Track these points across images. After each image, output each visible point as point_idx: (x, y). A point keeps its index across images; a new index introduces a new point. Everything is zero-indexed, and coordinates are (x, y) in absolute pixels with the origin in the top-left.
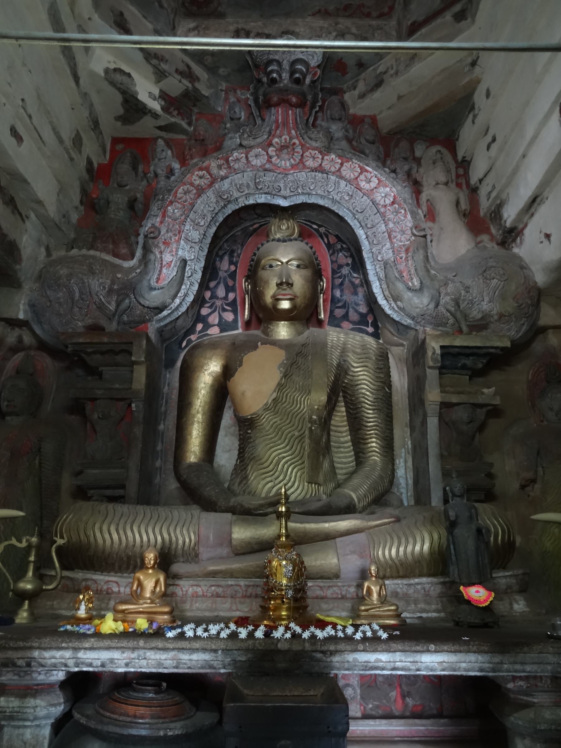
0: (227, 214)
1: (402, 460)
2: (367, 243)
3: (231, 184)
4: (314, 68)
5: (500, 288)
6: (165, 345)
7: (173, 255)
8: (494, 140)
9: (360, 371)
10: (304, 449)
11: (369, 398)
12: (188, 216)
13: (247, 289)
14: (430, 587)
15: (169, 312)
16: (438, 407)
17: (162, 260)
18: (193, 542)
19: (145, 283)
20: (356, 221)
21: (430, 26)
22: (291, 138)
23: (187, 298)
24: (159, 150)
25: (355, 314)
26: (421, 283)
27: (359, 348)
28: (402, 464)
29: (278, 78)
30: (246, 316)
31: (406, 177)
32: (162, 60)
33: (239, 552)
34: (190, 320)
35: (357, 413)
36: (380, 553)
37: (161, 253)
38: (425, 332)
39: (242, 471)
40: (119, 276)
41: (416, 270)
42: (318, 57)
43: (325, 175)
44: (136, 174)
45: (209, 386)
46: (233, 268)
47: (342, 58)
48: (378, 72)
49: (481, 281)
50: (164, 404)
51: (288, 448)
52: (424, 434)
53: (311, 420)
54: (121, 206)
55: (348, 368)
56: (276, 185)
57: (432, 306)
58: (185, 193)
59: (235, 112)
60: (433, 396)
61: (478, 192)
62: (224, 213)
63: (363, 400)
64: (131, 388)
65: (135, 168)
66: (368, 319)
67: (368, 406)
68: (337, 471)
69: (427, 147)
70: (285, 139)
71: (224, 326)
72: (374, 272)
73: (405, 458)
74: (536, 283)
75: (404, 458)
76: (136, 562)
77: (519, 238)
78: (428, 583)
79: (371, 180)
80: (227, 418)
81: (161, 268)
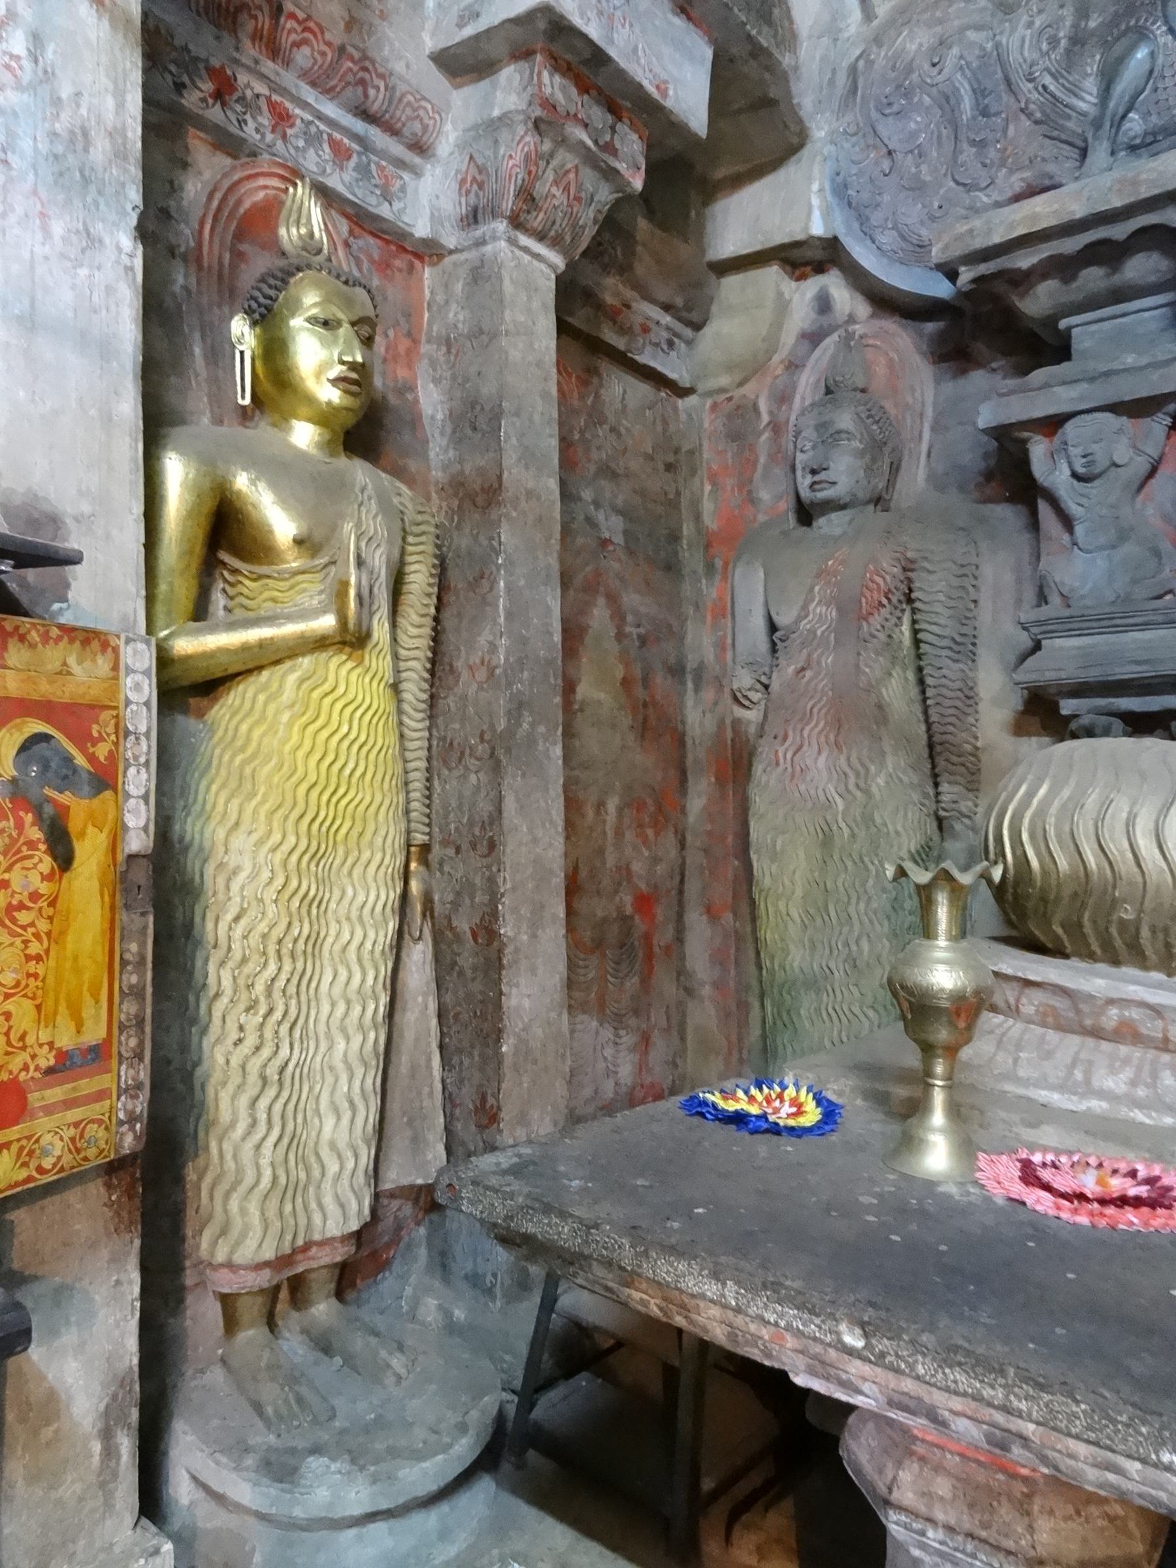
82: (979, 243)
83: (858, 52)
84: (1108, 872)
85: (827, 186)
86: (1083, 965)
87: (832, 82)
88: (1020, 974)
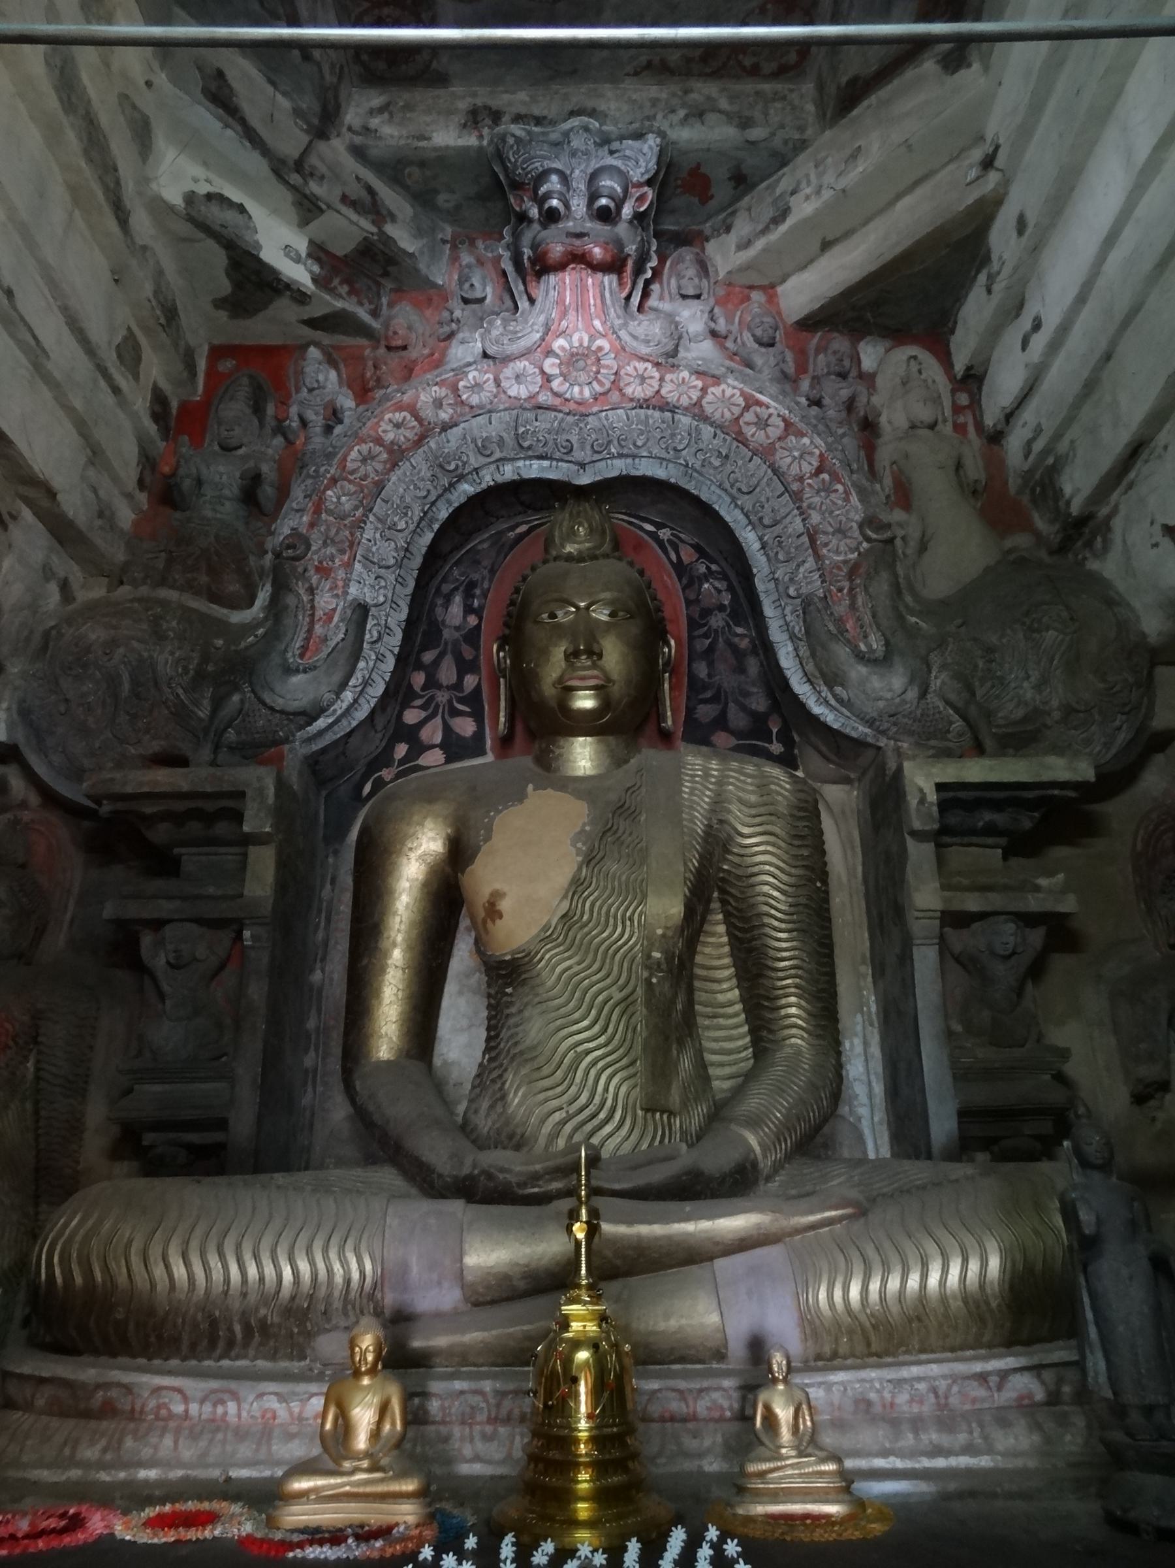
0: (456, 505)
1: (857, 1042)
2: (764, 559)
3: (465, 438)
4: (639, 185)
5: (1063, 648)
6: (324, 793)
7: (337, 596)
8: (1037, 326)
9: (757, 845)
10: (635, 1029)
11: (779, 906)
12: (371, 510)
13: (503, 666)
14: (949, 1387)
15: (330, 720)
16: (938, 922)
17: (313, 608)
18: (369, 1280)
19: (275, 659)
20: (737, 512)
21: (890, 87)
22: (592, 339)
23: (369, 690)
24: (310, 369)
25: (742, 714)
26: (887, 644)
27: (752, 792)
28: (859, 1049)
29: (562, 208)
30: (501, 727)
31: (844, 414)
32: (312, 175)
33: (481, 1299)
34: (380, 735)
35: (754, 939)
36: (822, 1295)
37: (311, 591)
38: (898, 752)
39: (493, 1081)
40: (220, 642)
41: (874, 616)
42: (648, 163)
43: (668, 414)
44: (262, 424)
45: (418, 884)
46: (473, 620)
47: (699, 165)
48: (778, 191)
49: (1021, 635)
50: (322, 924)
51: (597, 1028)
52: (908, 985)
54: (226, 492)
55: (730, 839)
56: (560, 439)
57: (912, 694)
58: (364, 460)
59: (472, 285)
60: (926, 897)
61: (1004, 442)
62: (449, 502)
63: (766, 908)
64: (241, 896)
65: (258, 409)
66: (771, 725)
67: (776, 923)
68: (711, 1071)
69: (888, 351)
70: (581, 340)
71: (455, 748)
72: (782, 622)
73: (864, 1037)
74: (1144, 635)
75: (861, 1035)
76: (230, 1330)
77: (1099, 539)
78: (944, 1377)
79: (769, 422)
81: (312, 623)
82: (117, 789)
83: (52, 623)
84: (109, 1284)
85: (14, 707)
86: (92, 1359)
87: (28, 640)
88: (36, 1373)
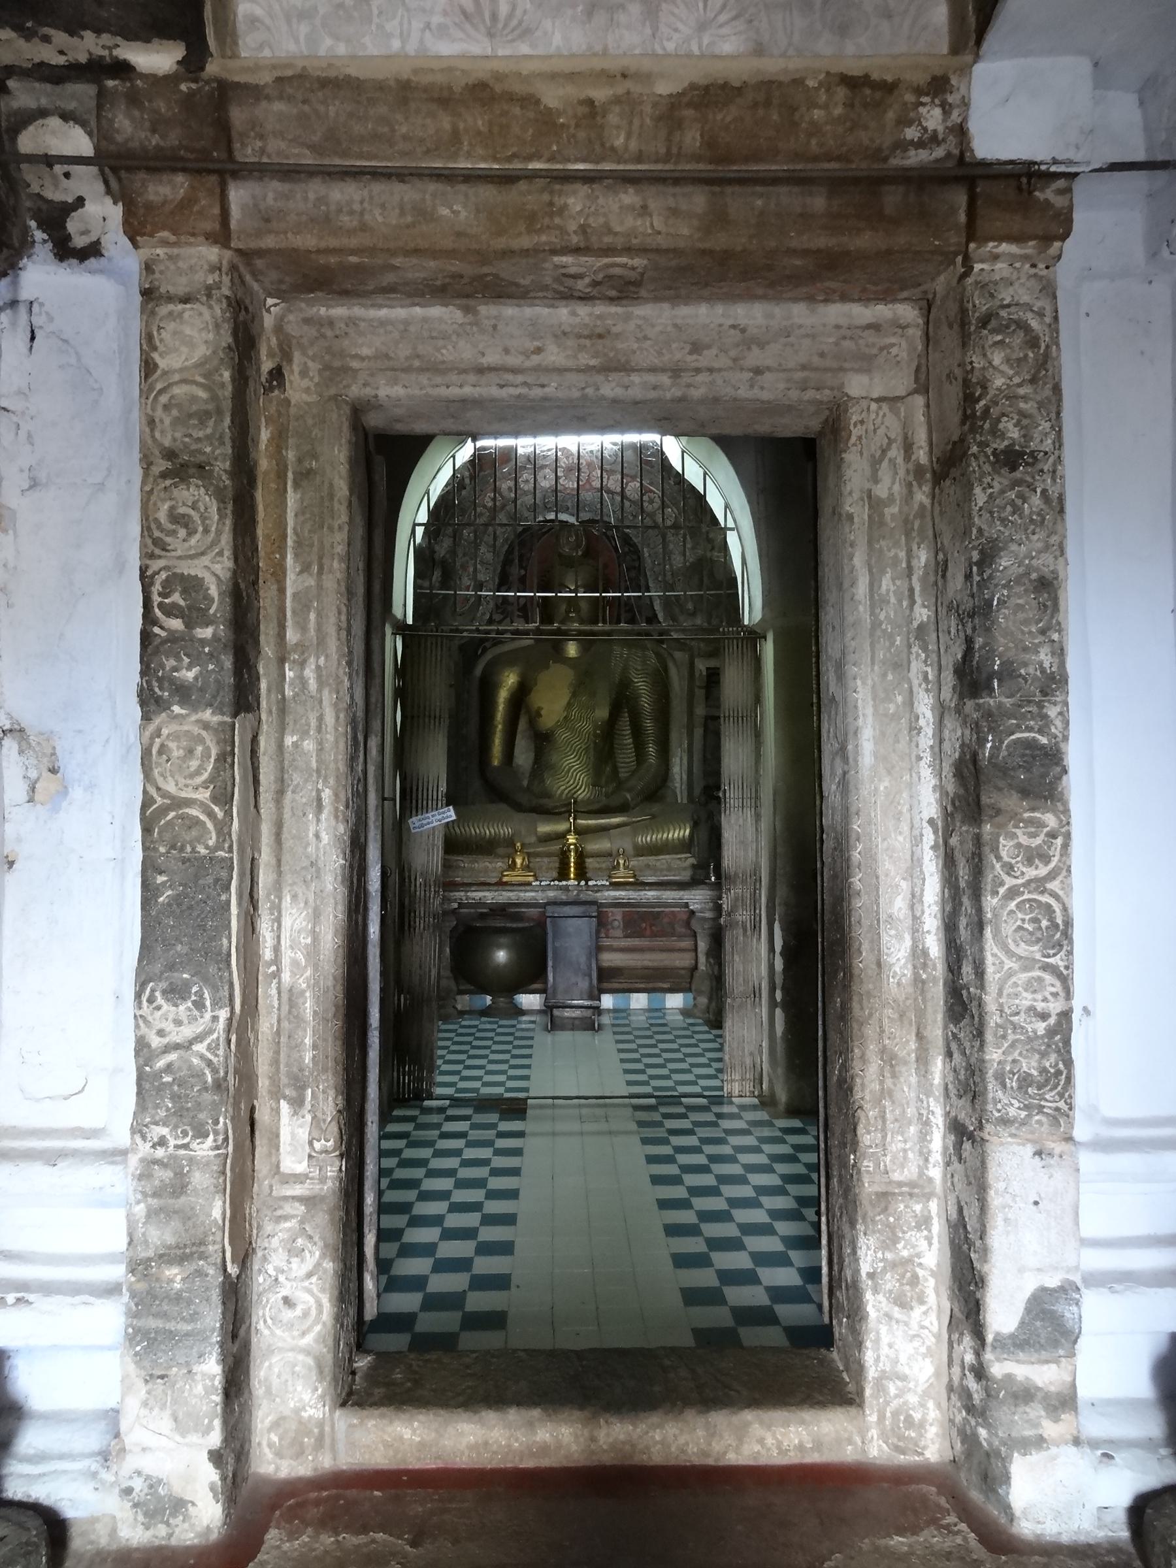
53: (596, 735)
80: (522, 725)
